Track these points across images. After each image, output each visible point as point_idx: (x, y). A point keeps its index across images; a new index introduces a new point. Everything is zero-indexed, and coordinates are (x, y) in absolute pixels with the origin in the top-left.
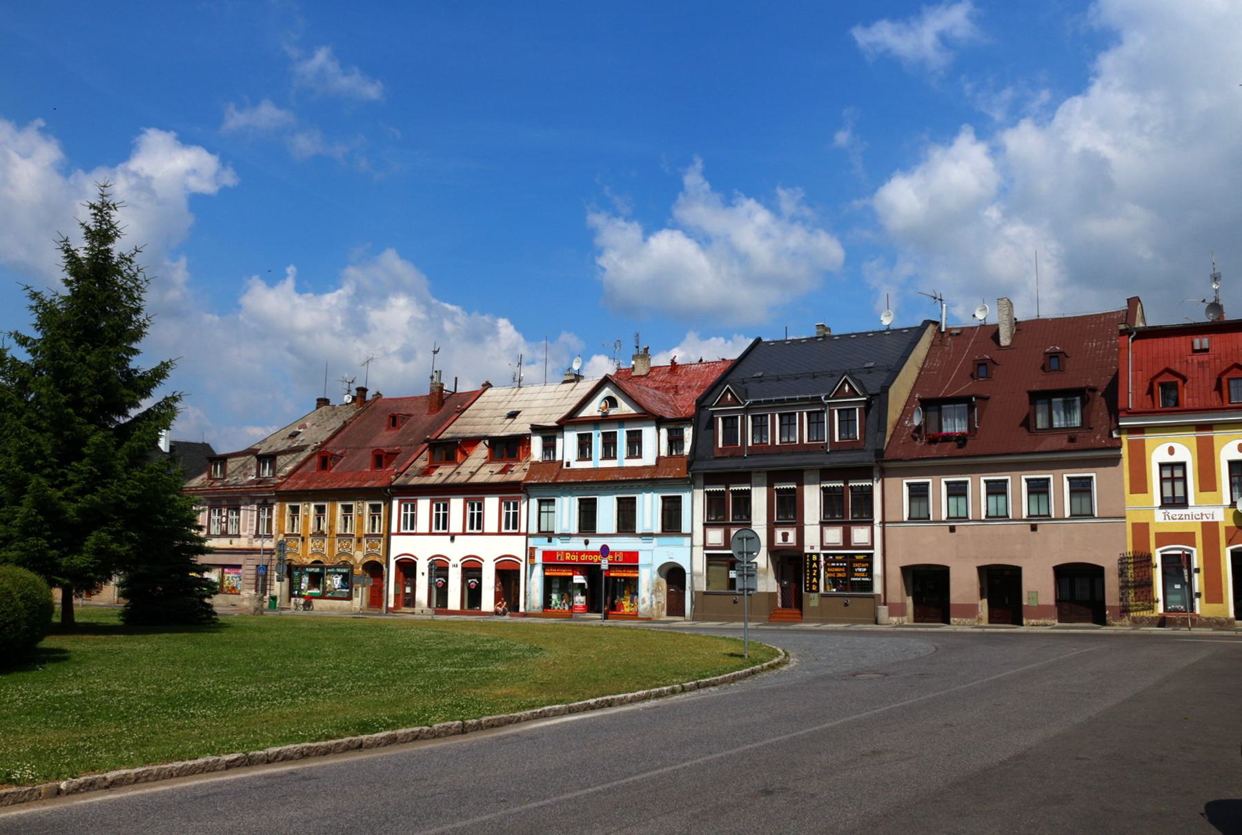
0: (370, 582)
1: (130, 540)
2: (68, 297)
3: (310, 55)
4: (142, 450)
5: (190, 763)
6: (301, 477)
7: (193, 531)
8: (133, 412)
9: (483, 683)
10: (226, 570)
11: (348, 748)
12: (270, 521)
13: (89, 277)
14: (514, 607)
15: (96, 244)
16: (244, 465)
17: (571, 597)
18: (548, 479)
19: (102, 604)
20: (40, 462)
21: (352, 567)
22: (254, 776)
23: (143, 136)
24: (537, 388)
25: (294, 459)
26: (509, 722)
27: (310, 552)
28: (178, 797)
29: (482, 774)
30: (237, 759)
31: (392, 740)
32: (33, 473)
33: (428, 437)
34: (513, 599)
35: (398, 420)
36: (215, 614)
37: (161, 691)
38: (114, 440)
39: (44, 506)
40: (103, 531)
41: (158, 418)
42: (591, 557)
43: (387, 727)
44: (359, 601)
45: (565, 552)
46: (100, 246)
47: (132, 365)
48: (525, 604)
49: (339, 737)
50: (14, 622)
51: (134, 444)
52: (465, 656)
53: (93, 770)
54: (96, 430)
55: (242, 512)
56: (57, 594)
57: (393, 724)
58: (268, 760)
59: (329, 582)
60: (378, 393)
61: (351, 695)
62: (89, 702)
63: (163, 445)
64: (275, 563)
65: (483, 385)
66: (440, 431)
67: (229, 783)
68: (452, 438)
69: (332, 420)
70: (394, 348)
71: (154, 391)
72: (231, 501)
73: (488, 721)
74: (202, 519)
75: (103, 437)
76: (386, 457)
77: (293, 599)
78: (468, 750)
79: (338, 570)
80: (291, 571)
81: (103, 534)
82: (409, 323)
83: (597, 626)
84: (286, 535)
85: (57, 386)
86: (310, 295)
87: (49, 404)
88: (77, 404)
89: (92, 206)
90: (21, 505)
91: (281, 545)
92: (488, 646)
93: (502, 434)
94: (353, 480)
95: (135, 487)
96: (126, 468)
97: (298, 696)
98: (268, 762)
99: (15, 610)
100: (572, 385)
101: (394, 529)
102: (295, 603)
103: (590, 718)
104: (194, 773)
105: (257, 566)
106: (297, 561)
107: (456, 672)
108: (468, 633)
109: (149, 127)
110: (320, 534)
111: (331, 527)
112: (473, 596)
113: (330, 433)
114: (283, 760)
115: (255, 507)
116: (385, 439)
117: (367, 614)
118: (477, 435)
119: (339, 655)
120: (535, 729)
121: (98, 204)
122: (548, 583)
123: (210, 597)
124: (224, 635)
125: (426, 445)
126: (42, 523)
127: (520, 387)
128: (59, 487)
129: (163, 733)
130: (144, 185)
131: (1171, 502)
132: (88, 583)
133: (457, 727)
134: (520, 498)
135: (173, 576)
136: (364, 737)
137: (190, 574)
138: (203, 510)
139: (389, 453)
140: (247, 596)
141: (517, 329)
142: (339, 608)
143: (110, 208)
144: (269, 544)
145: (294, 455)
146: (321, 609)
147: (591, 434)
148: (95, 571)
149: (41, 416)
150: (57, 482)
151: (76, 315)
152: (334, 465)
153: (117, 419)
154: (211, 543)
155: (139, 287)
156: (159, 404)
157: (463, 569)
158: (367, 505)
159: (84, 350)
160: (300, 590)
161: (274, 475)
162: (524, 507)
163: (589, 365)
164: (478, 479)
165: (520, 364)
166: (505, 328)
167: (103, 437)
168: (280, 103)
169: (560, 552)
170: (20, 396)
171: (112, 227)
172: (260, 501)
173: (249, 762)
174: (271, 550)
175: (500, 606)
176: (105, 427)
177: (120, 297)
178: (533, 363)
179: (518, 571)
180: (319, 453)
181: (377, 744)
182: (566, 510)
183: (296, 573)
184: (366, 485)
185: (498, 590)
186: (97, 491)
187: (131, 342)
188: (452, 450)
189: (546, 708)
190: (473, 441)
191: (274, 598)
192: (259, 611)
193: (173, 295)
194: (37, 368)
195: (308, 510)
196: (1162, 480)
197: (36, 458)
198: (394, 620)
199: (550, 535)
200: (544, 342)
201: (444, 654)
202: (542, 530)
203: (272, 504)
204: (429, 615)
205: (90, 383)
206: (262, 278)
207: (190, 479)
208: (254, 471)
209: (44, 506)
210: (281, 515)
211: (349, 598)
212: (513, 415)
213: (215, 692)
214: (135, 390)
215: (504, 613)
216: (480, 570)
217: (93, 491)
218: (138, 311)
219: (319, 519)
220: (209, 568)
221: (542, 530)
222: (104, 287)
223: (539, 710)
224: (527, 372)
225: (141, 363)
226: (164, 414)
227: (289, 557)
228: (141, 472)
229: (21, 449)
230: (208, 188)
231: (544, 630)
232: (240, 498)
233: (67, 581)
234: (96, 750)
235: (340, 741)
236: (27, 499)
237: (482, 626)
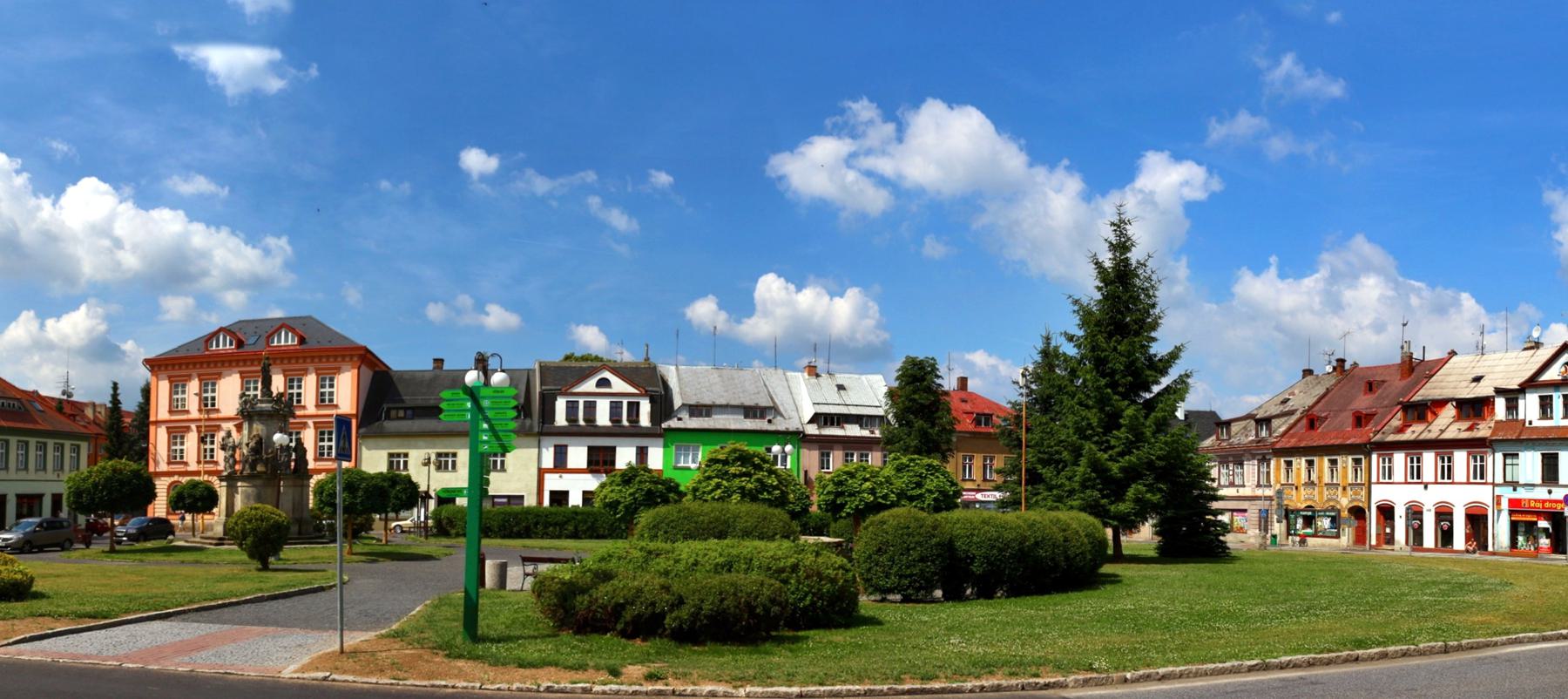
0: (1355, 523)
1: (1160, 490)
2: (1100, 301)
3: (1278, 63)
4: (1165, 418)
5: (1221, 665)
6: (1292, 436)
7: (1207, 482)
8: (1156, 389)
9: (1459, 612)
10: (1235, 514)
11: (1347, 661)
12: (1268, 473)
13: (1116, 282)
14: (1483, 546)
15: (1118, 254)
16: (1245, 428)
17: (1536, 539)
18: (1511, 435)
19: (1140, 540)
20: (1090, 432)
21: (1339, 511)
22: (1272, 679)
23: (1144, 158)
24: (1498, 355)
25: (1286, 421)
26: (1487, 645)
27: (1303, 498)
28: (1212, 691)
29: (1466, 689)
30: (1257, 665)
31: (1384, 656)
32: (1086, 440)
33: (1401, 399)
34: (1482, 540)
35: (1374, 387)
36: (1229, 549)
37: (1192, 609)
38: (1143, 412)
39: (1096, 466)
40: (1140, 484)
41: (1175, 392)
42: (1554, 505)
43: (1379, 644)
44: (1346, 538)
45: (1530, 500)
46: (1121, 255)
47: (1152, 351)
48: (1493, 544)
49: (1338, 650)
50: (1081, 553)
51: (1159, 415)
52: (1442, 587)
53: (1148, 666)
54: (1129, 405)
55: (1245, 466)
56: (1109, 532)
57: (1384, 642)
58: (1282, 667)
59: (1319, 523)
60: (1355, 363)
61: (1346, 617)
62: (1140, 615)
63: (1180, 414)
64: (1275, 507)
65: (1449, 353)
66: (1411, 395)
67: (1252, 683)
68: (1422, 400)
69: (1316, 388)
70: (1366, 322)
71: (1171, 371)
72: (1236, 458)
73: (1468, 643)
74: (1214, 473)
75: (1135, 410)
76: (1365, 418)
77: (1290, 537)
78: (1452, 667)
79: (1328, 514)
80: (1288, 514)
81: (1139, 486)
82: (1379, 300)
83: (1563, 566)
84: (1282, 485)
85: (1097, 373)
86: (1290, 280)
87: (1093, 386)
88: (1113, 385)
89: (1113, 224)
90: (1079, 465)
91: (1279, 492)
92: (1462, 579)
93: (1468, 397)
94: (1338, 438)
95: (1161, 449)
96: (1154, 434)
97: (1301, 616)
98: (1282, 668)
99: (1082, 545)
100: (1532, 351)
101: (1374, 479)
102: (1293, 541)
103: (1563, 647)
104: (1223, 674)
105: (1260, 510)
106: (1292, 506)
107: (1435, 601)
108: (1443, 568)
109: (1147, 150)
110: (1310, 484)
111: (1320, 478)
112: (1446, 537)
113: (1315, 399)
114: (1293, 667)
115: (1256, 462)
116: (1363, 402)
117: (1354, 550)
118: (1444, 397)
119: (1333, 584)
120: (1512, 653)
121: (1117, 222)
122: (1514, 527)
123: (1224, 535)
124: (1237, 566)
125: (1399, 406)
126: (1095, 479)
127: (1483, 354)
128: (1105, 451)
129: (1197, 641)
130: (1149, 199)
132: (1128, 524)
133: (1440, 647)
134: (1486, 453)
135: (1194, 518)
136: (1360, 652)
137: (1207, 517)
138: (1215, 466)
139: (1366, 415)
140: (1252, 535)
141: (1478, 302)
142: (1329, 545)
143: (1126, 224)
144: (1269, 492)
145: (1286, 418)
146: (1314, 546)
147: (1551, 397)
148: (1135, 514)
149: (1088, 396)
150: (1103, 447)
151: (1108, 314)
152: (1321, 425)
153: (1144, 395)
154: (1221, 493)
155: (1153, 286)
156: (1175, 381)
157: (1436, 513)
158: (1350, 458)
159: (1116, 342)
160: (1296, 530)
161: (1270, 435)
162: (1490, 459)
163: (1547, 332)
164: (1447, 435)
165: (1482, 333)
166: (1467, 301)
167: (1135, 410)
168: (1254, 112)
169: (1525, 500)
170: (1072, 381)
171: (1129, 239)
172: (1260, 457)
173: (1266, 667)
174: (1270, 497)
175: (1470, 545)
176: (1134, 402)
177: (1139, 296)
178: (1494, 331)
179: (1487, 516)
180: (1307, 416)
181: (1371, 658)
182: (1529, 464)
183: (1292, 516)
184: (1348, 442)
185: (1468, 531)
186: (1133, 453)
187: (1151, 332)
188: (1422, 411)
189: (1521, 635)
190: (1441, 403)
191: (1274, 536)
192: (1263, 546)
193: (1178, 289)
194: (1082, 358)
195: (1300, 464)
197: (1087, 429)
198: (1377, 556)
199: (1515, 485)
200: (1503, 313)
201: (1423, 585)
202: (1507, 480)
203: (1270, 459)
204: (1407, 551)
205: (1122, 368)
206: (1250, 268)
207: (1203, 440)
208: (1254, 432)
209: (1096, 466)
210: (1278, 468)
211: (1338, 536)
212: (1477, 379)
213: (1235, 611)
214: (1156, 371)
215: (1474, 552)
216: (1451, 514)
217: (1130, 453)
218: (1153, 306)
219: (1309, 471)
220: (1222, 512)
221: (1507, 480)
222: (1126, 290)
223: (1514, 637)
224: (1489, 340)
225: (1159, 349)
226: (1180, 389)
227: (1285, 502)
228: (1165, 436)
229: (1076, 423)
230: (1199, 195)
231: (1512, 568)
232: (1243, 455)
233: (1116, 523)
234: (1149, 651)
235: (1340, 654)
236: (1083, 461)
237: (1455, 562)
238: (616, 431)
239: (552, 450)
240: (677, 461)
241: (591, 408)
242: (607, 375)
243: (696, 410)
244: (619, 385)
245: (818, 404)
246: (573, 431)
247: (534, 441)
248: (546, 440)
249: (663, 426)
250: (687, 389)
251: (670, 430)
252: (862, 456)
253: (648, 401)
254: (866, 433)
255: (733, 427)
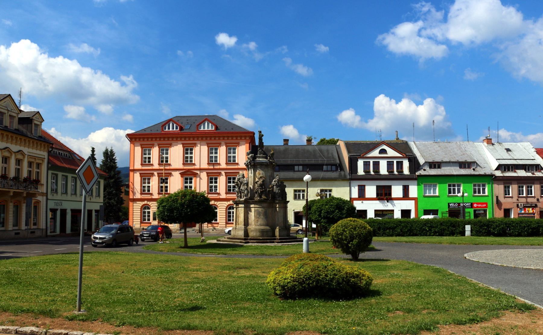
238: (391, 177)
239: (357, 188)
240: (425, 193)
241: (377, 165)
242: (384, 147)
243: (433, 165)
244: (391, 152)
245: (499, 159)
246: (368, 177)
247: (347, 183)
248: (353, 183)
249: (417, 174)
250: (424, 154)
251: (421, 176)
252: (528, 187)
253: (408, 161)
254: (529, 174)
255: (455, 173)
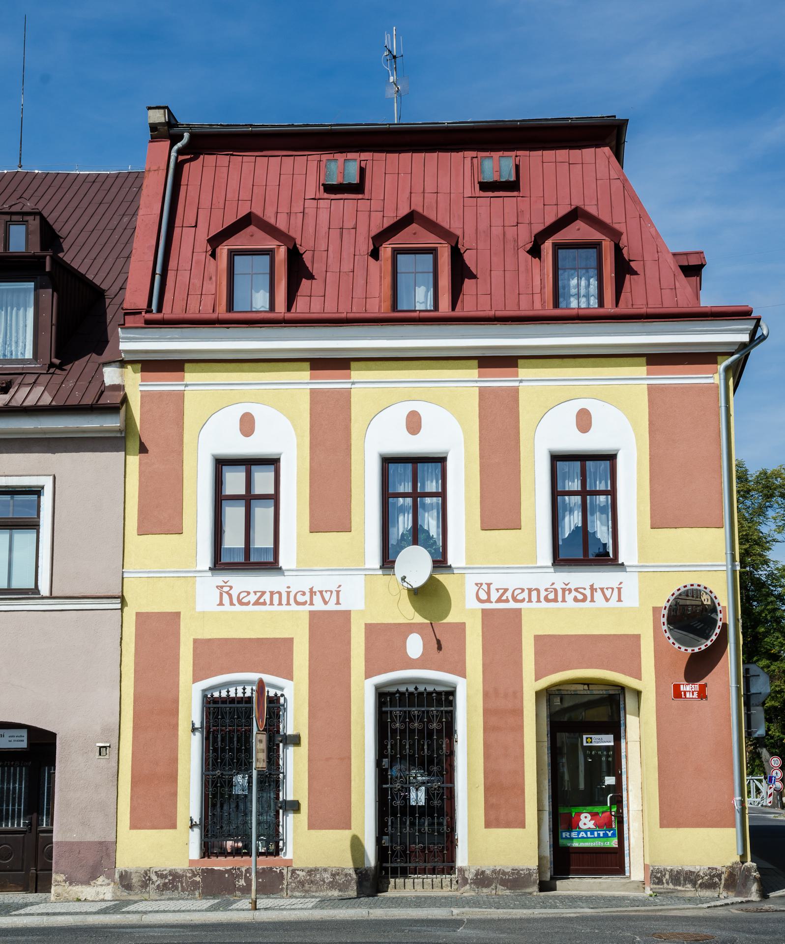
131: (241, 559)
196: (220, 499)
